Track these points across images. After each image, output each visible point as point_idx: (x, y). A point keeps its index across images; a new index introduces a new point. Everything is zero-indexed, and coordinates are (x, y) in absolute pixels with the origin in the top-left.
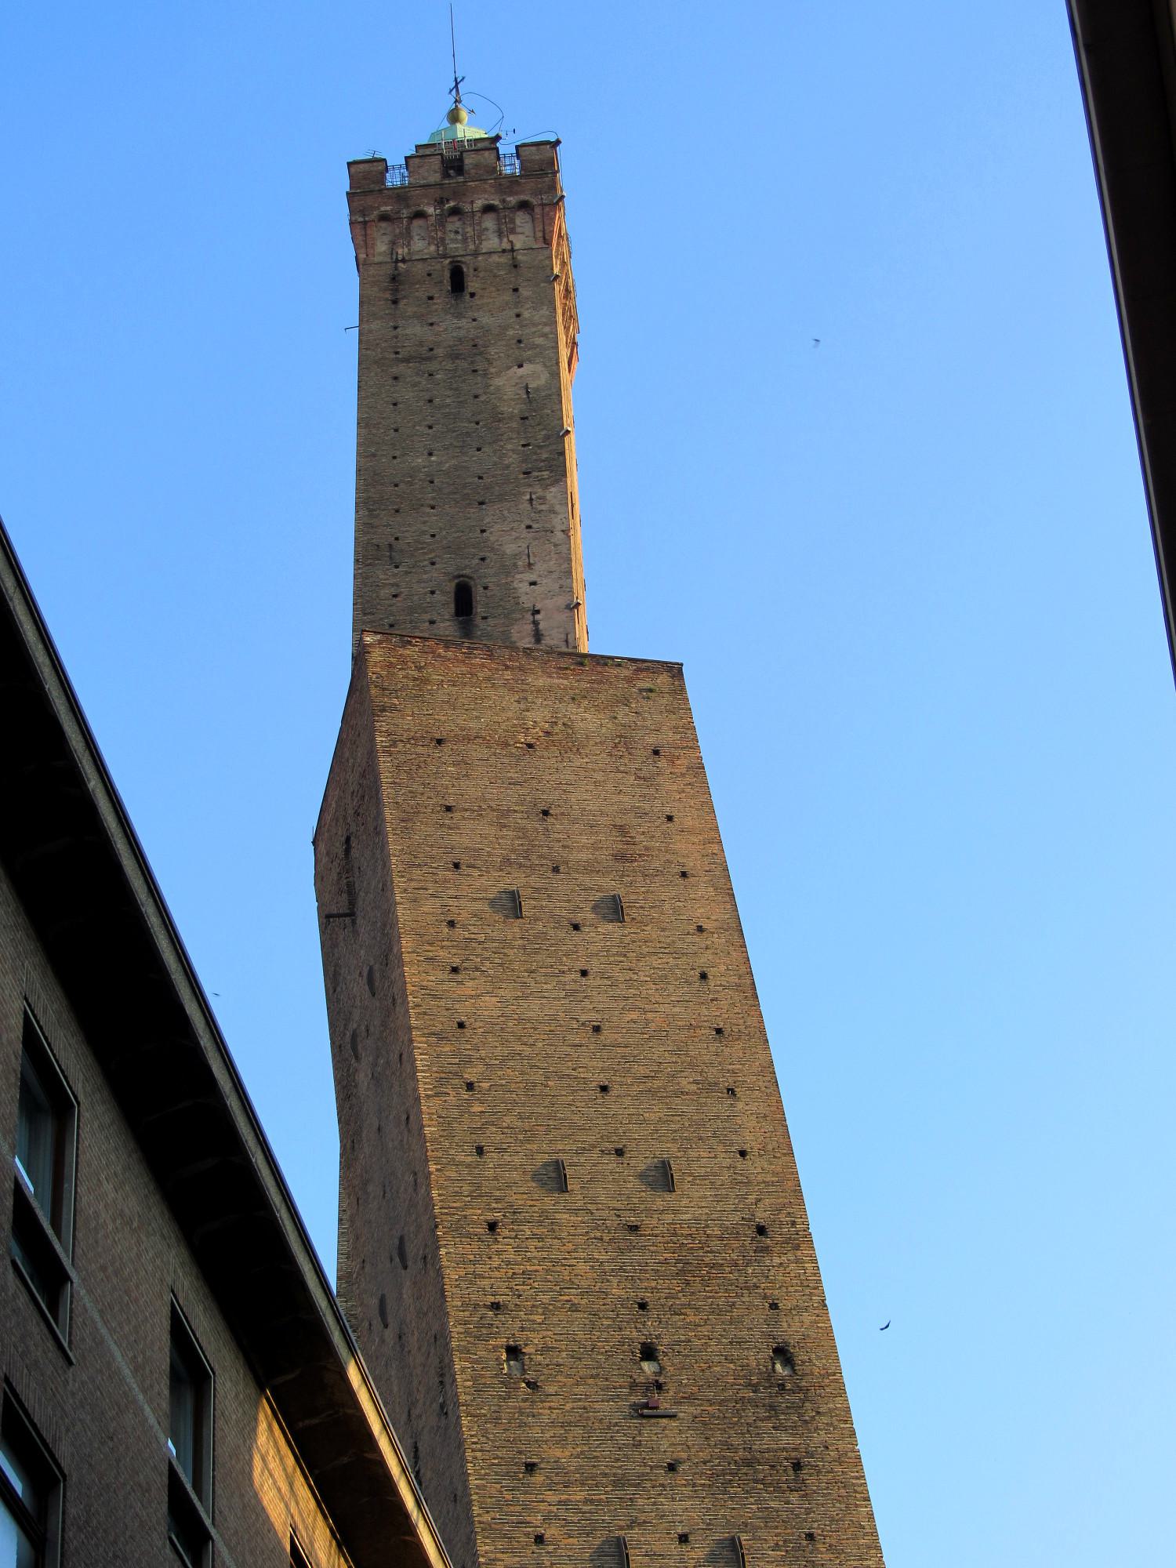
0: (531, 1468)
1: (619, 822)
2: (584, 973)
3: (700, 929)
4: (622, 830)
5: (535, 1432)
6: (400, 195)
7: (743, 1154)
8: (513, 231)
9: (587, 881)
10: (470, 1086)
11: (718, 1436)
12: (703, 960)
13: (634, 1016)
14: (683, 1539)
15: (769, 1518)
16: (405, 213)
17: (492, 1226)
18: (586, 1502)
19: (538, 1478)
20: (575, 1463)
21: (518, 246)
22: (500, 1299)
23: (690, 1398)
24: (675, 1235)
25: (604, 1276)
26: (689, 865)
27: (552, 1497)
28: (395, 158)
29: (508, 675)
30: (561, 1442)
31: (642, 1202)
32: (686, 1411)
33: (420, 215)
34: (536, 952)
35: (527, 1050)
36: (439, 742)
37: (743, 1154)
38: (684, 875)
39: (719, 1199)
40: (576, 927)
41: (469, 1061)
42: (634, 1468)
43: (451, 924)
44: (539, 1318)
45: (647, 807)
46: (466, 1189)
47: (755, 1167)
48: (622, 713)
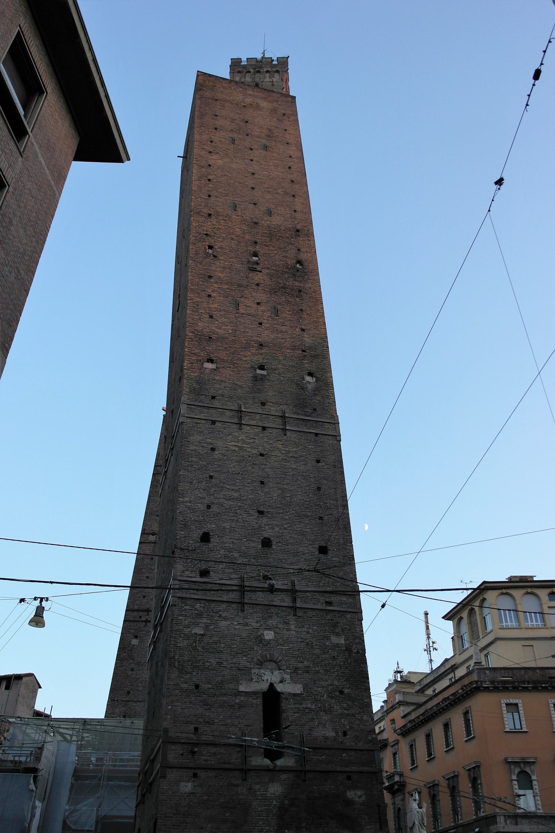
0: (210, 277)
1: (269, 128)
2: (252, 160)
3: (291, 157)
4: (270, 130)
5: (214, 268)
6: (244, 67)
7: (295, 211)
8: (273, 77)
9: (257, 140)
10: (210, 180)
11: (275, 279)
12: (290, 164)
13: (266, 173)
14: (258, 304)
15: (288, 302)
16: (245, 71)
17: (210, 215)
18: (227, 289)
19: (212, 280)
20: (225, 278)
21: (274, 81)
22: (208, 233)
23: (268, 268)
24: (269, 227)
25: (244, 233)
26: (290, 141)
27: (216, 286)
28: (244, 59)
29: (241, 89)
30: (222, 272)
31: (260, 217)
32: (265, 271)
33: (249, 72)
34: (237, 153)
35: (230, 175)
36: (216, 100)
37: (295, 211)
38: (288, 143)
39: (285, 221)
40: (251, 149)
41: (211, 174)
42: (244, 283)
43: (211, 142)
44: (220, 240)
45: (279, 126)
46: (203, 204)
47: (298, 215)
48: (275, 104)
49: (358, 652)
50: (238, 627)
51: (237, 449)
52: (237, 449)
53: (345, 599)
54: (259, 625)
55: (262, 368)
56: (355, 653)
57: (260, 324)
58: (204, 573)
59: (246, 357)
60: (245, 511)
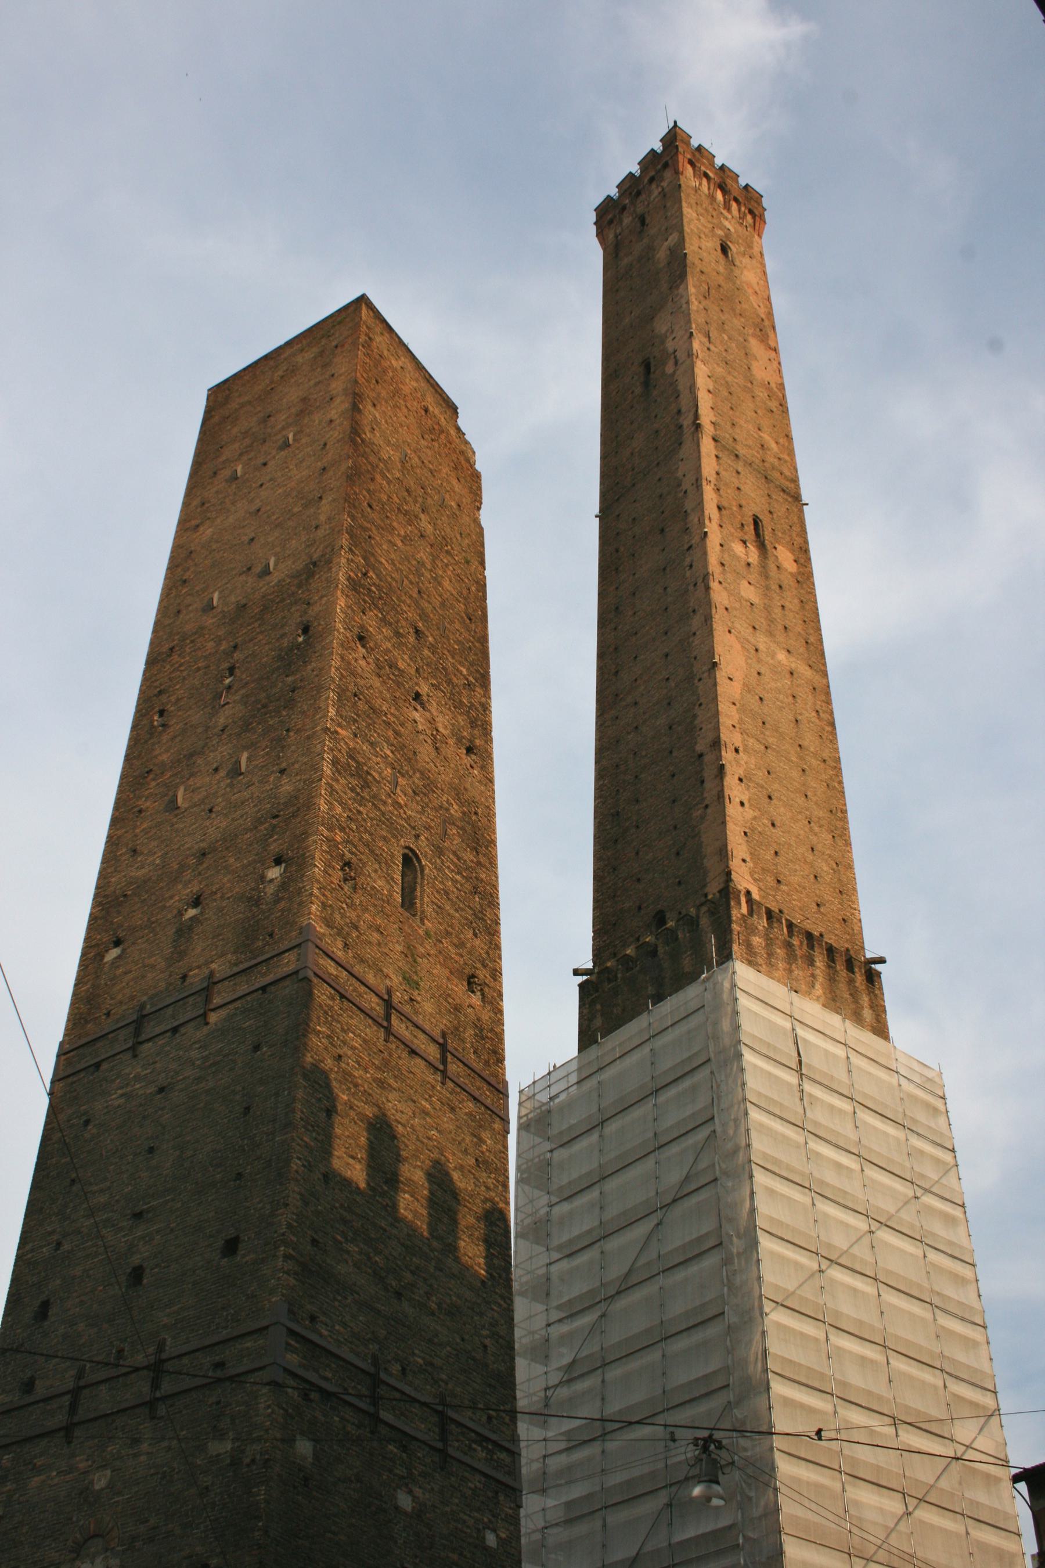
14: (216, 770)
19: (151, 776)
27: (153, 784)
33: (624, 208)
49: (253, 1461)
50: (56, 1481)
51: (122, 1101)
52: (122, 1101)
53: (249, 1344)
54: (90, 1463)
55: (196, 902)
56: (248, 1465)
57: (211, 811)
58: (29, 1386)
59: (171, 897)
60: (113, 1225)
